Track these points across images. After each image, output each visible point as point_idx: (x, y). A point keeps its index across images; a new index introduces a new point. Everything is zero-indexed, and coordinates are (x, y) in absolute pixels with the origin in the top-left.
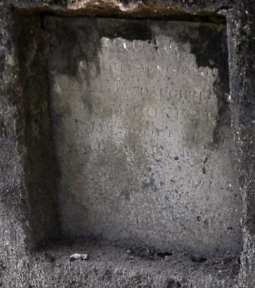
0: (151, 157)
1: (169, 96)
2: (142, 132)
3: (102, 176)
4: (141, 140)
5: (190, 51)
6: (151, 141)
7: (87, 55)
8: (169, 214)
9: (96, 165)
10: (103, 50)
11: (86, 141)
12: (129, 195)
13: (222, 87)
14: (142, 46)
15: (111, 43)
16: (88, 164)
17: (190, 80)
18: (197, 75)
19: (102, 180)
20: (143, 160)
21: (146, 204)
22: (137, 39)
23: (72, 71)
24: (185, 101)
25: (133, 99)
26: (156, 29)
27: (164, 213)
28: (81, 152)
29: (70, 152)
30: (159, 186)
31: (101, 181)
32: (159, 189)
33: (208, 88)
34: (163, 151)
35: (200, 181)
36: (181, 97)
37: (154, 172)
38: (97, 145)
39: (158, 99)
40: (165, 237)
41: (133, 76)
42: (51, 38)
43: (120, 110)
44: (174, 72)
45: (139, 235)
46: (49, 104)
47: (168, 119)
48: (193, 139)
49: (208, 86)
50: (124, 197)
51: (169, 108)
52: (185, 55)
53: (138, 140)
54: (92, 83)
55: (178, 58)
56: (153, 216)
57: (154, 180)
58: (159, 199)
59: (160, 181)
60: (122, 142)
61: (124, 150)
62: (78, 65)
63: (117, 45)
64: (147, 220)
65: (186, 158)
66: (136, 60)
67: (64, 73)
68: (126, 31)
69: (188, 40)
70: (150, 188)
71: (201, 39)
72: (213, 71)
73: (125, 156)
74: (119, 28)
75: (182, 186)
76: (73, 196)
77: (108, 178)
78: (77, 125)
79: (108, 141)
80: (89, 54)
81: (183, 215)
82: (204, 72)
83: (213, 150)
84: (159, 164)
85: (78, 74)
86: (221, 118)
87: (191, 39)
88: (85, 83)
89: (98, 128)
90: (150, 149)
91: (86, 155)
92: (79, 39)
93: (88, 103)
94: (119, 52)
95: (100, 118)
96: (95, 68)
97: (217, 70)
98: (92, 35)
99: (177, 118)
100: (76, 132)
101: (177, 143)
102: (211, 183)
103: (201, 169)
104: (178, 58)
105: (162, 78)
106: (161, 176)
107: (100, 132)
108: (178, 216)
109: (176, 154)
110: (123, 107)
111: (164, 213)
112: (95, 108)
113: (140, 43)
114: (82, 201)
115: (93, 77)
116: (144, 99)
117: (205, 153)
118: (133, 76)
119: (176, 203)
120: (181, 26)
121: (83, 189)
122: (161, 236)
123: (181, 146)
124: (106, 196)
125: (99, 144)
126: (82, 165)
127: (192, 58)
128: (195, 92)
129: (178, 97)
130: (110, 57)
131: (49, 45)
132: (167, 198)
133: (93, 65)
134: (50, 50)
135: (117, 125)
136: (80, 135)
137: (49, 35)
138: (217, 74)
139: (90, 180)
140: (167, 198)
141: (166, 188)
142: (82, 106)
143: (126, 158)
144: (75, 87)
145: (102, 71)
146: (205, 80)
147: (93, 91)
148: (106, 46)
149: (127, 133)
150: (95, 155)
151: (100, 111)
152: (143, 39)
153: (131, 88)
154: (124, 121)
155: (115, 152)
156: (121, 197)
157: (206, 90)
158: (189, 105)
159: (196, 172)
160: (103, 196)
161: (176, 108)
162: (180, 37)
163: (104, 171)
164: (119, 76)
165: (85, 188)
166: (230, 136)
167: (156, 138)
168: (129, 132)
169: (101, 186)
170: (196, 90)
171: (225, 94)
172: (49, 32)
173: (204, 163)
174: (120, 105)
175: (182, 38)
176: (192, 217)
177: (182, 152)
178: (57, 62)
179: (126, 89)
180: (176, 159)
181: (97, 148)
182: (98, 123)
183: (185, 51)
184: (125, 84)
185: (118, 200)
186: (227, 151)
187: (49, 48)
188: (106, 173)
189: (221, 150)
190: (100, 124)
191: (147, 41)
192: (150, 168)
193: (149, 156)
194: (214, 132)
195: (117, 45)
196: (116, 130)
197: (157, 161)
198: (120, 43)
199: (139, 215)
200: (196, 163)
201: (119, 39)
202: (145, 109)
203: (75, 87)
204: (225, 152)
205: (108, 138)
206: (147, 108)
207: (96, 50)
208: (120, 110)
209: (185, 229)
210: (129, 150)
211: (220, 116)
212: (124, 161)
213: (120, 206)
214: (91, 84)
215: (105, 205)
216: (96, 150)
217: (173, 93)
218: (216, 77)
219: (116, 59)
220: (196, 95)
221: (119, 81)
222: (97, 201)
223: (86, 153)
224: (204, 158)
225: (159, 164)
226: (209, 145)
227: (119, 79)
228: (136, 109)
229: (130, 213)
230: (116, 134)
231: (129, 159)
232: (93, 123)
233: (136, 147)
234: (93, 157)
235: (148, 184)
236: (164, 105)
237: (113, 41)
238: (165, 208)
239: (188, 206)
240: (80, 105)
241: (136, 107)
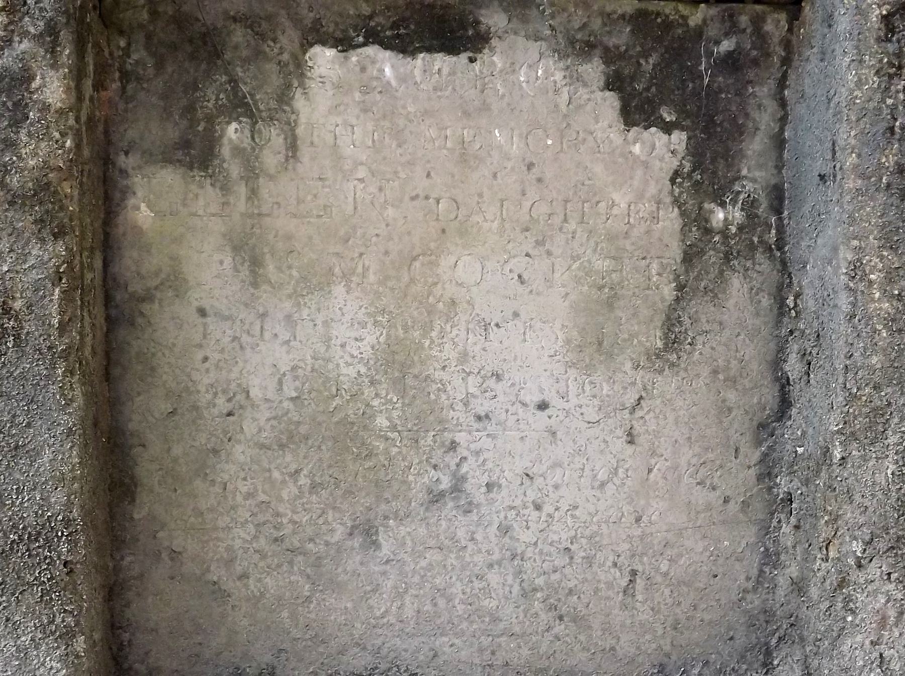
0: (460, 406)
1: (528, 217)
2: (434, 334)
3: (284, 482)
4: (430, 357)
5: (602, 83)
6: (464, 357)
7: (256, 103)
8: (510, 579)
9: (262, 446)
10: (313, 85)
11: (233, 376)
12: (377, 532)
13: (697, 184)
14: (445, 71)
15: (341, 65)
16: (239, 448)
17: (599, 169)
18: (622, 155)
19: (285, 495)
20: (431, 418)
21: (433, 556)
22: (429, 50)
23: (196, 153)
24: (579, 230)
25: (409, 233)
27: (494, 578)
28: (216, 411)
29: (173, 413)
30: (479, 496)
31: (280, 500)
32: (478, 506)
33: (652, 190)
34: (499, 387)
35: (616, 469)
36: (565, 220)
37: (465, 453)
38: (272, 385)
39: (490, 230)
40: (493, 653)
41: (411, 163)
42: (127, 52)
43: (360, 270)
44: (548, 147)
45: (407, 655)
46: (106, 264)
47: (520, 289)
48: (600, 344)
49: (653, 183)
50: (357, 542)
51: (527, 255)
52: (586, 97)
53: (416, 358)
54: (266, 188)
55: (563, 107)
56: (457, 589)
57: (464, 479)
58: (479, 537)
59: (485, 479)
60: (363, 370)
61: (368, 392)
62: (221, 137)
63: (363, 69)
64: (435, 605)
65: (574, 401)
66: (426, 113)
67: (167, 160)
68: (395, 26)
69: (598, 52)
70: (451, 504)
71: (638, 49)
72: (670, 139)
73: (368, 414)
74: (371, 17)
75: (556, 487)
76: (175, 555)
77: (306, 489)
78: (205, 325)
79: (313, 370)
80: (264, 100)
81: (555, 577)
82: (643, 143)
83: (661, 372)
84: (485, 429)
85: (216, 162)
86: (692, 275)
87: (607, 50)
88: (242, 190)
89: (278, 329)
90: (457, 382)
91: (231, 418)
92: (228, 56)
94: (366, 89)
95: (290, 296)
96: (281, 140)
97: (684, 136)
98: (274, 40)
99: (549, 282)
100: (200, 346)
101: (546, 359)
102: (650, 471)
103: (619, 432)
104: (563, 107)
105: (509, 165)
106: (489, 465)
107: (287, 342)
108: (540, 581)
109: (541, 390)
110: (371, 261)
111: (494, 578)
112: (271, 267)
113: (441, 61)
114: (208, 570)
115: (272, 171)
116: (443, 231)
117: (634, 384)
118: (411, 163)
119: (536, 544)
121: (216, 529)
122: (481, 650)
123: (558, 369)
124: (297, 544)
125: (280, 383)
126: (215, 452)
127: (611, 102)
128: (613, 204)
129: (557, 220)
130: (335, 109)
131: (117, 75)
132: (505, 530)
133: (275, 137)
134: (124, 88)
135: (348, 317)
136: (215, 356)
137: (122, 43)
138: (681, 148)
139: (239, 498)
140: (505, 530)
141: (502, 497)
142: (228, 261)
143: (372, 417)
144: (207, 205)
145: (305, 153)
146: (646, 165)
147: (268, 215)
148: (323, 71)
149: (382, 339)
150: (264, 414)
151: (291, 276)
152: (452, 50)
153: (401, 201)
154: (372, 304)
155: (337, 401)
156: (350, 543)
157: (648, 195)
158: (592, 243)
159: (605, 441)
160: (287, 544)
161: (549, 253)
162: (572, 42)
163: (293, 467)
164: (362, 164)
165: (221, 524)
166: (716, 327)
167: (477, 348)
168: (388, 336)
169: (278, 515)
170: (616, 197)
171: (706, 206)
172: (121, 33)
173: (633, 410)
174: (361, 255)
176: (585, 580)
177: (562, 384)
178: (149, 127)
179: (384, 207)
180: (543, 406)
181: (270, 395)
182: (280, 316)
183: (585, 85)
184: (381, 189)
185: (338, 551)
186: (705, 371)
187: (116, 85)
188: (297, 472)
189: (686, 370)
190: (288, 317)
191: (464, 57)
192: (453, 442)
193: (451, 407)
194: (668, 318)
195: (363, 69)
196: (341, 332)
197: (479, 418)
198: (373, 62)
200: (607, 416)
201: (372, 51)
202: (446, 262)
203: (207, 205)
204: (698, 376)
205: (315, 358)
206: (453, 259)
207: (289, 86)
208: (360, 270)
209: (561, 618)
210: (383, 393)
211: (687, 271)
212: (365, 427)
213: (345, 571)
214: (264, 193)
215: (291, 573)
216: (267, 400)
217: (543, 209)
218: (679, 157)
219: (357, 111)
220: (615, 211)
221: (361, 180)
222: (262, 564)
223: (230, 414)
224: (630, 398)
225: (485, 429)
226: (649, 359)
227: (362, 173)
228: (417, 264)
229: (374, 591)
230: (343, 346)
231: (381, 421)
232: (263, 316)
233: (410, 381)
234: (256, 424)
235: (442, 494)
236: (510, 246)
237: (346, 58)
238: (499, 563)
239: (573, 548)
240: (221, 262)
241: (415, 259)
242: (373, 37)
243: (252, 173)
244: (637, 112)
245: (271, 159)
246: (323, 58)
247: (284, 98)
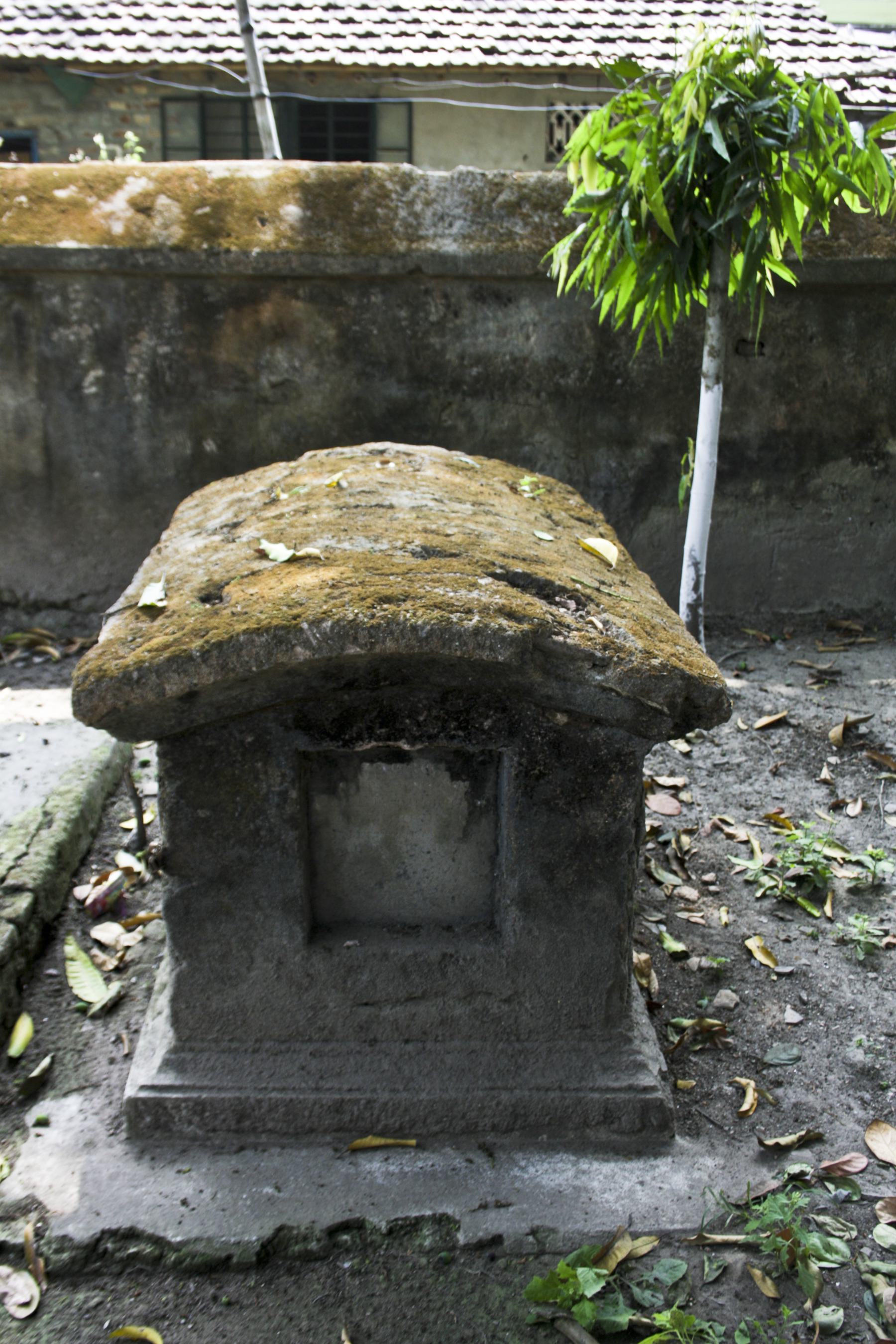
113: (399, 766)
242: (380, 760)
244: (455, 776)
245: (352, 791)
246: (366, 766)
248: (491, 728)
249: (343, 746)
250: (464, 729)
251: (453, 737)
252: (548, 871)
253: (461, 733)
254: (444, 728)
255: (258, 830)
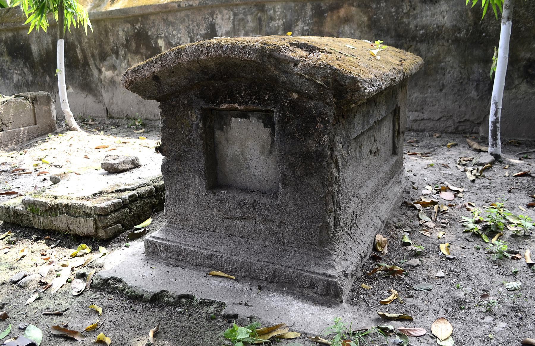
26: (250, 115)
93: (227, 140)
113: (245, 119)
120: (259, 114)
175: (259, 118)
199: (245, 178)
234: (229, 158)
243: (227, 131)
245: (229, 130)
246: (233, 119)
247: (230, 123)
248: (268, 99)
249: (216, 105)
250: (258, 99)
251: (254, 103)
252: (292, 166)
253: (257, 101)
254: (251, 99)
255: (189, 139)
